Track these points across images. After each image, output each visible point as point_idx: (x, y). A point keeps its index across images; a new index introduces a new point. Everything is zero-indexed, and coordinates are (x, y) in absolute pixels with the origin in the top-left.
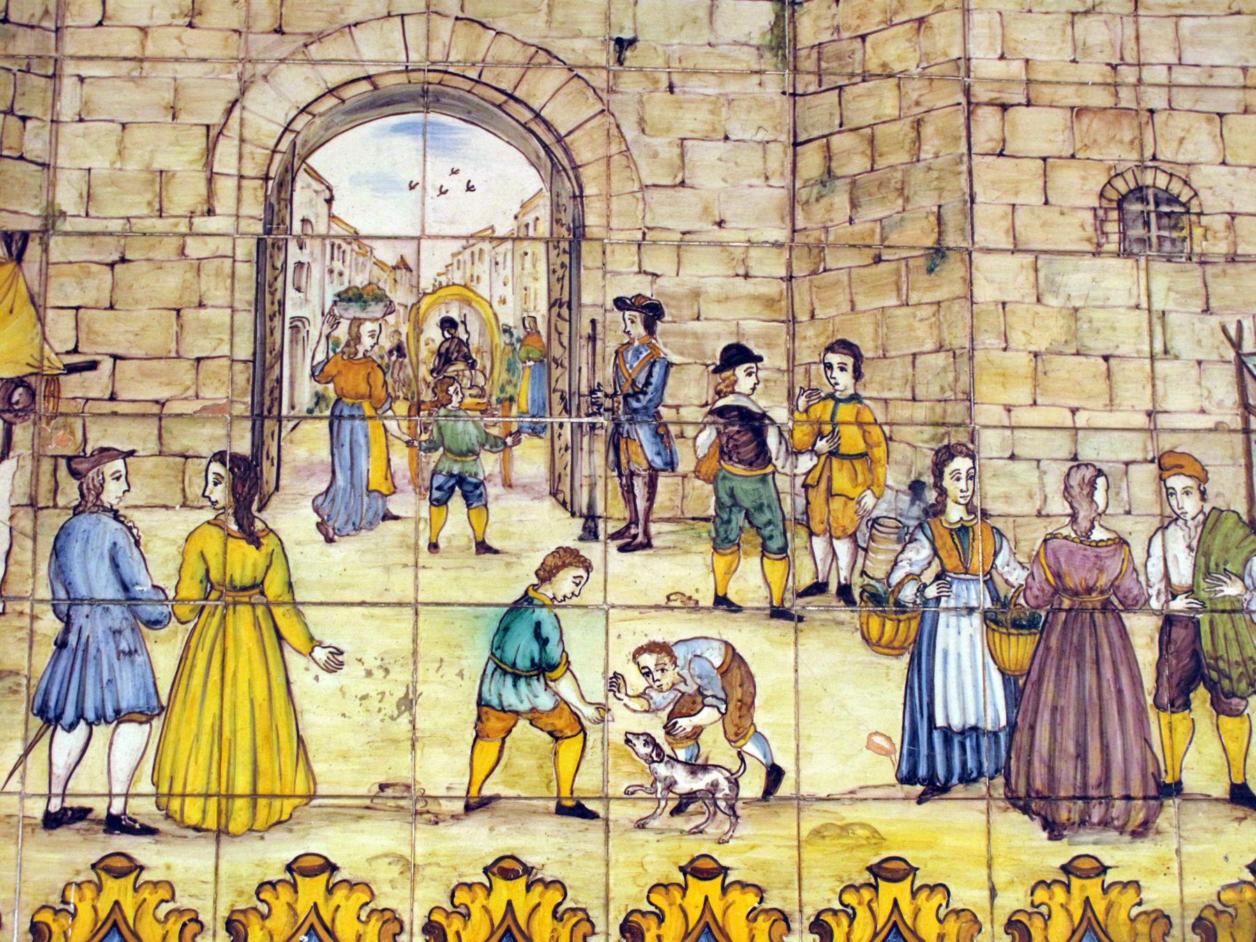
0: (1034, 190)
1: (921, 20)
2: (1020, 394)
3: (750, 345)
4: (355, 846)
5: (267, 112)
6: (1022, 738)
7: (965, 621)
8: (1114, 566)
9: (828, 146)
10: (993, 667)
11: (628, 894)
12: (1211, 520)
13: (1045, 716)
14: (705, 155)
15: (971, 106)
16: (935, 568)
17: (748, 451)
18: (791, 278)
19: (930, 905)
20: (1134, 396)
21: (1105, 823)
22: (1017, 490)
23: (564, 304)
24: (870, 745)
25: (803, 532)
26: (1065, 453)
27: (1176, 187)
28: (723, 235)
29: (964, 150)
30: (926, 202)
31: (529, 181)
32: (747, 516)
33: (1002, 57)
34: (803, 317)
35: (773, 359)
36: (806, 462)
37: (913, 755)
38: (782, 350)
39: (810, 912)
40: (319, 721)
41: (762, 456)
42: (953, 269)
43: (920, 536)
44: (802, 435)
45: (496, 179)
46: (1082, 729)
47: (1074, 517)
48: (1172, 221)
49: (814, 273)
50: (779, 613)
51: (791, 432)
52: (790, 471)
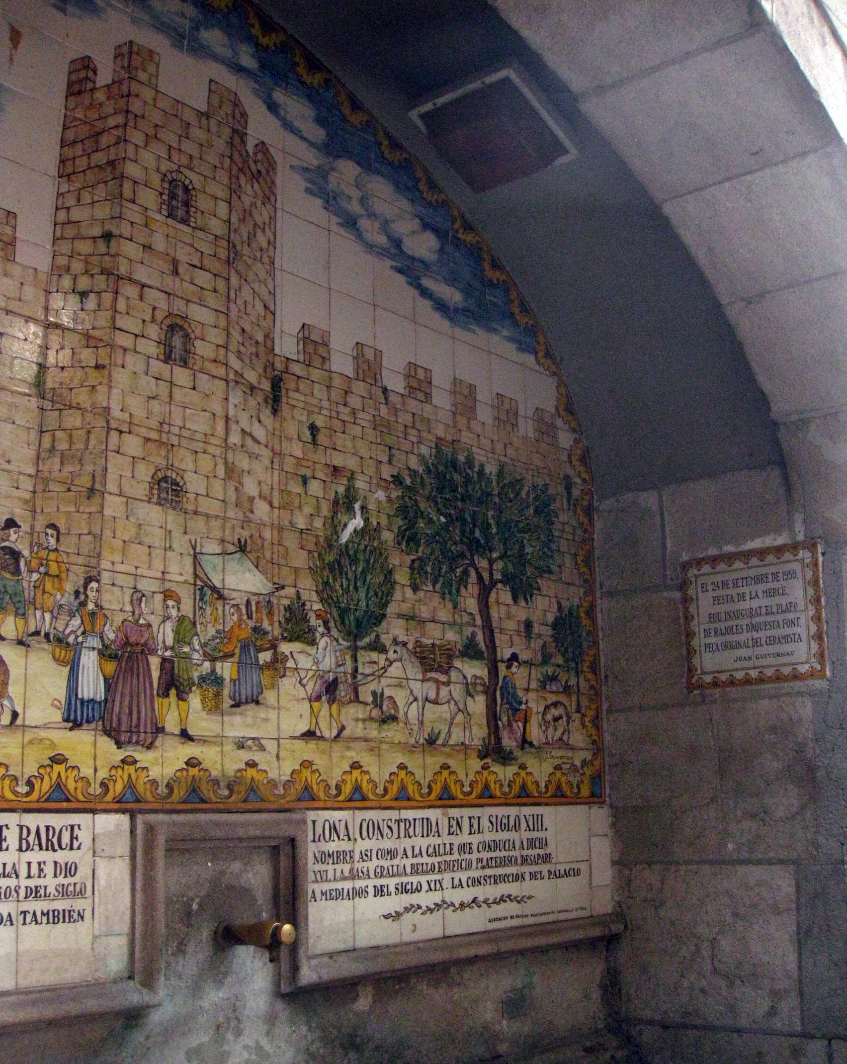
1: (93, 387)
2: (118, 558)
3: (17, 520)
6: (109, 705)
7: (91, 653)
8: (146, 635)
9: (54, 436)
10: (100, 673)
12: (181, 620)
13: (118, 697)
15: (109, 429)
16: (82, 629)
17: (12, 568)
18: (34, 492)
19: (72, 774)
20: (158, 565)
21: (137, 743)
22: (115, 600)
24: (53, 705)
25: (32, 607)
26: (131, 585)
27: (179, 479)
28: (8, 467)
29: (104, 448)
30: (89, 468)
32: (10, 598)
33: (122, 410)
34: (39, 511)
35: (25, 527)
36: (35, 576)
37: (69, 709)
38: (28, 524)
39: (26, 777)
41: (17, 571)
42: (96, 499)
43: (77, 614)
44: (34, 564)
46: (131, 703)
47: (133, 612)
48: (177, 493)
49: (44, 491)
50: (20, 643)
51: (30, 562)
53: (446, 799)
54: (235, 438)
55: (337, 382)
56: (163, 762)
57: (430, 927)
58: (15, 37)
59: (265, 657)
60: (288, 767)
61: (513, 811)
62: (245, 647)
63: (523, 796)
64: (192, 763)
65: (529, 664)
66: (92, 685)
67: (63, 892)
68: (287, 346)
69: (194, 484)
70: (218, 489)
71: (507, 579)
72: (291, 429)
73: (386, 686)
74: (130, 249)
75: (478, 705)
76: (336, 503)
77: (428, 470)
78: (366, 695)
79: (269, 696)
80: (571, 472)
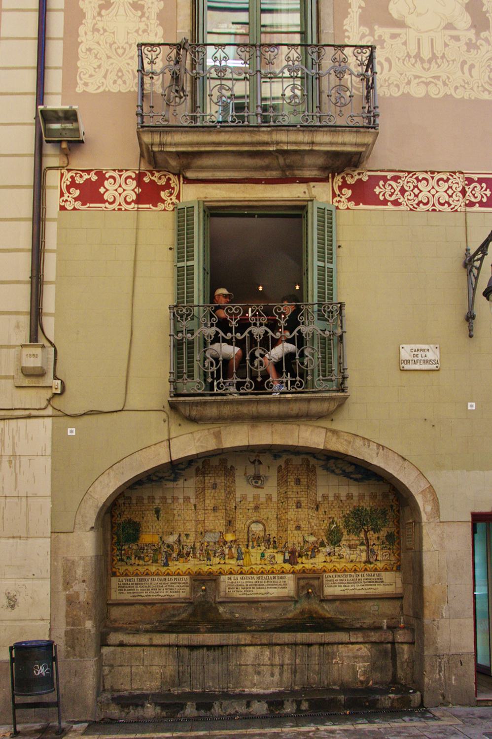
0: (291, 526)
4: (254, 567)
5: (248, 523)
11: (268, 569)
14: (273, 525)
22: (290, 545)
23: (265, 535)
31: (262, 527)
40: (252, 560)
45: (261, 527)
52: (277, 544)
54: (310, 517)
55: (330, 502)
56: (299, 567)
59: (316, 550)
60: (320, 567)
62: (312, 549)
64: (303, 567)
65: (378, 545)
66: (287, 557)
67: (284, 585)
68: (320, 499)
69: (302, 526)
70: (307, 526)
71: (372, 529)
72: (321, 513)
73: (341, 552)
74: (289, 493)
75: (364, 554)
76: (330, 523)
77: (351, 512)
78: (337, 554)
79: (317, 556)
80: (392, 504)
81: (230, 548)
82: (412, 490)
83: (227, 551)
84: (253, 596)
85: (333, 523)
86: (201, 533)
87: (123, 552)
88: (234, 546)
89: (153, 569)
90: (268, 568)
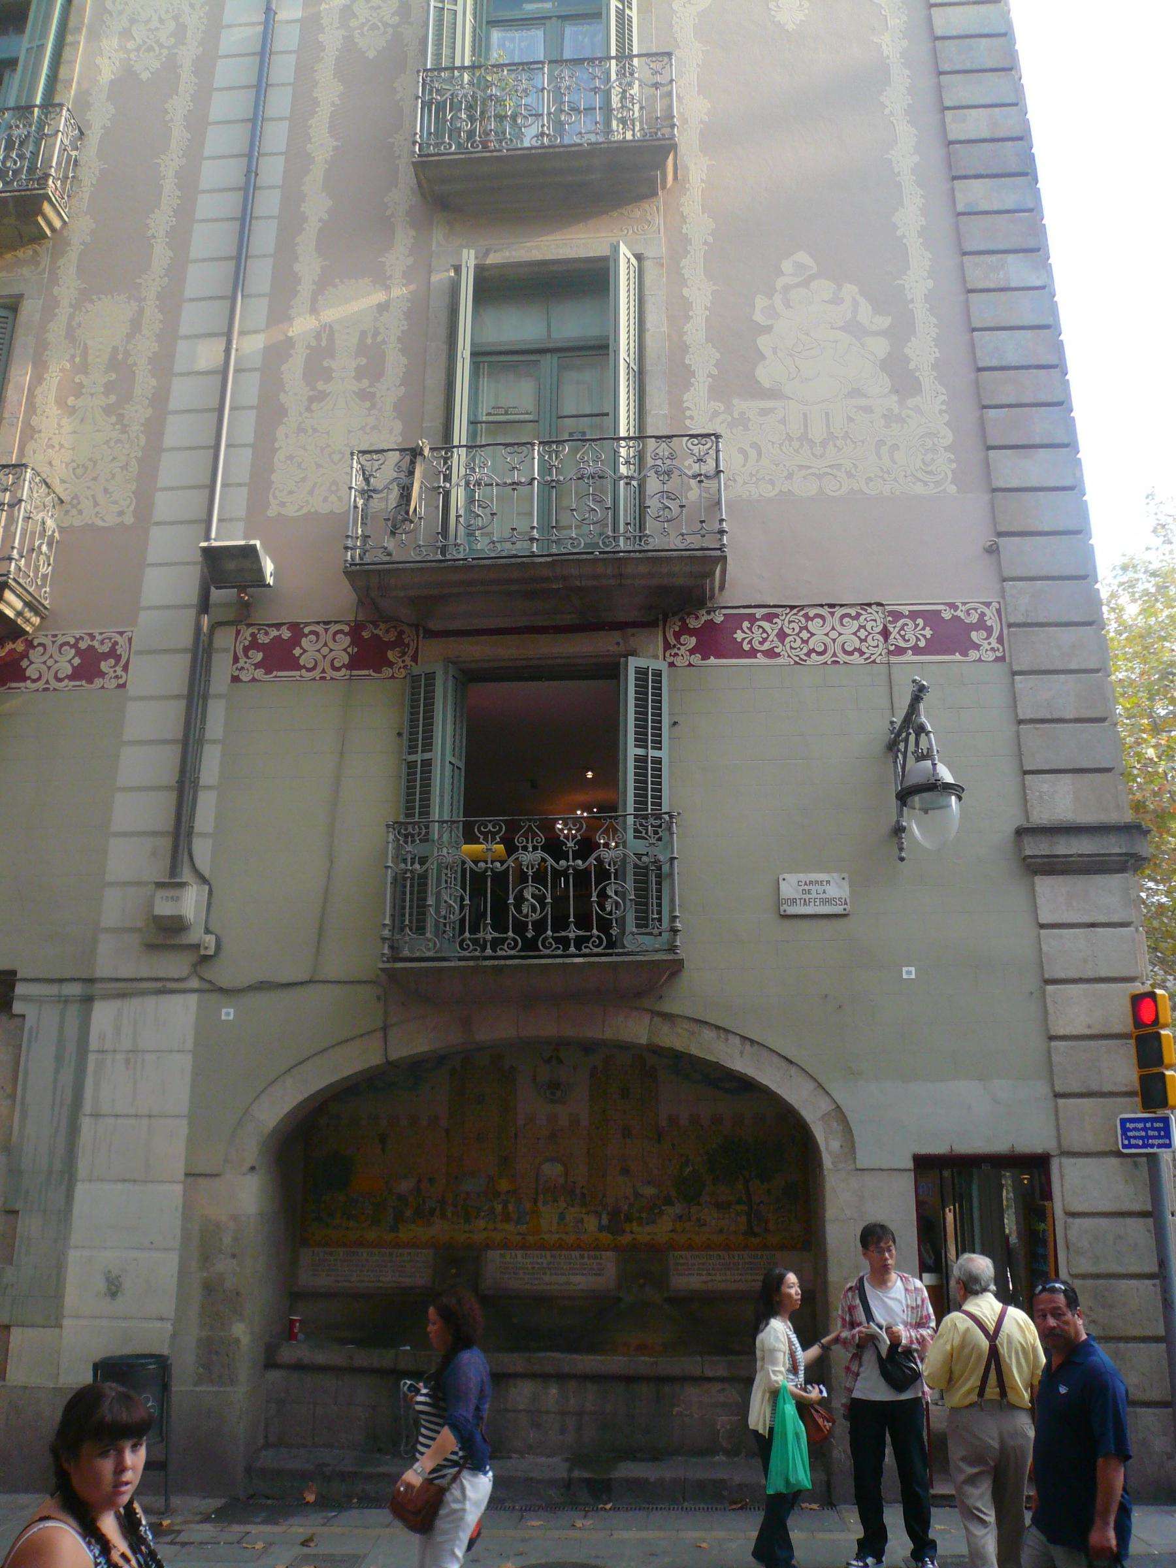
4: (546, 1237)
45: (559, 1168)
53: (727, 1247)
56: (625, 1239)
57: (721, 1286)
58: (575, 1068)
61: (759, 1253)
63: (765, 1247)
66: (605, 1220)
75: (744, 1219)
78: (694, 1218)
81: (505, 1207)
82: (804, 1113)
83: (499, 1208)
84: (545, 1287)
85: (687, 1165)
86: (456, 1178)
87: (323, 1206)
88: (512, 1201)
89: (371, 1235)
90: (571, 1239)
